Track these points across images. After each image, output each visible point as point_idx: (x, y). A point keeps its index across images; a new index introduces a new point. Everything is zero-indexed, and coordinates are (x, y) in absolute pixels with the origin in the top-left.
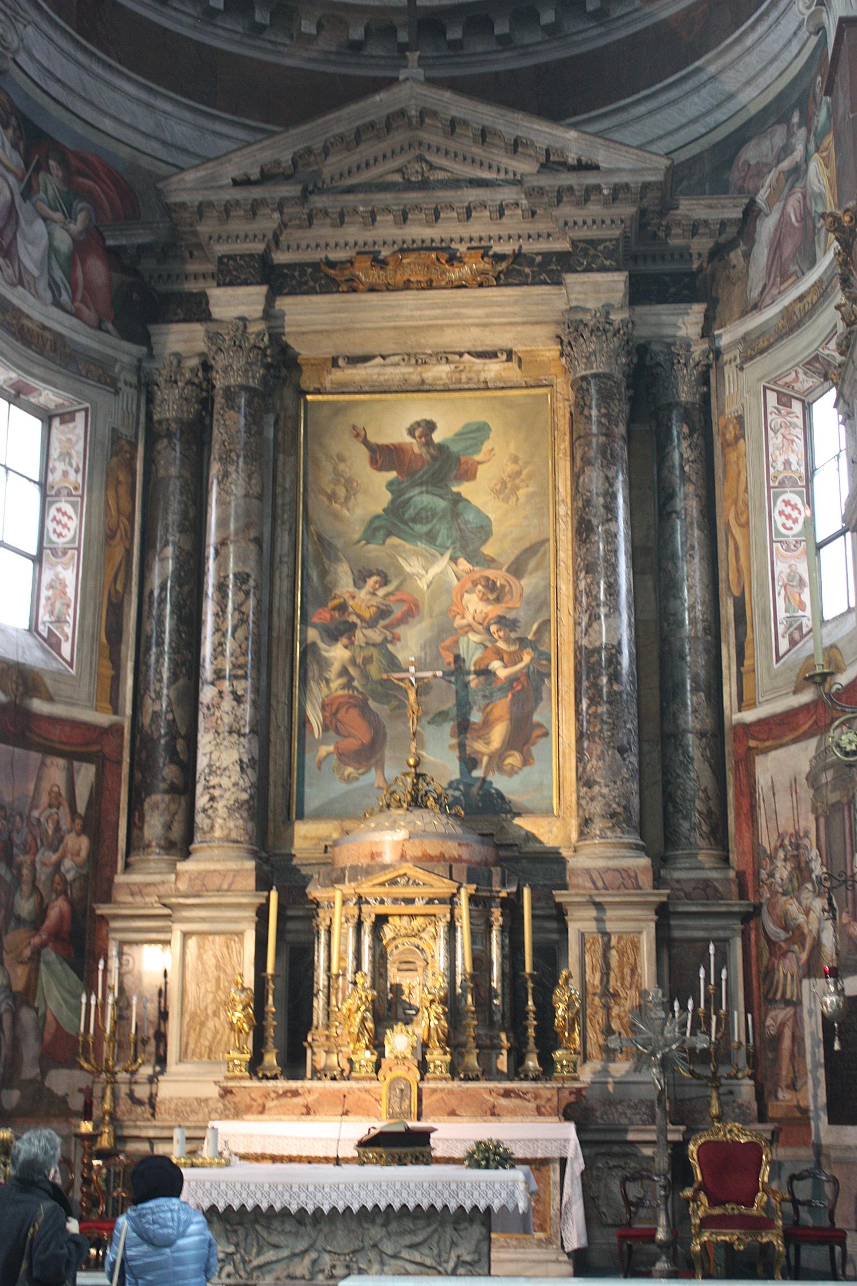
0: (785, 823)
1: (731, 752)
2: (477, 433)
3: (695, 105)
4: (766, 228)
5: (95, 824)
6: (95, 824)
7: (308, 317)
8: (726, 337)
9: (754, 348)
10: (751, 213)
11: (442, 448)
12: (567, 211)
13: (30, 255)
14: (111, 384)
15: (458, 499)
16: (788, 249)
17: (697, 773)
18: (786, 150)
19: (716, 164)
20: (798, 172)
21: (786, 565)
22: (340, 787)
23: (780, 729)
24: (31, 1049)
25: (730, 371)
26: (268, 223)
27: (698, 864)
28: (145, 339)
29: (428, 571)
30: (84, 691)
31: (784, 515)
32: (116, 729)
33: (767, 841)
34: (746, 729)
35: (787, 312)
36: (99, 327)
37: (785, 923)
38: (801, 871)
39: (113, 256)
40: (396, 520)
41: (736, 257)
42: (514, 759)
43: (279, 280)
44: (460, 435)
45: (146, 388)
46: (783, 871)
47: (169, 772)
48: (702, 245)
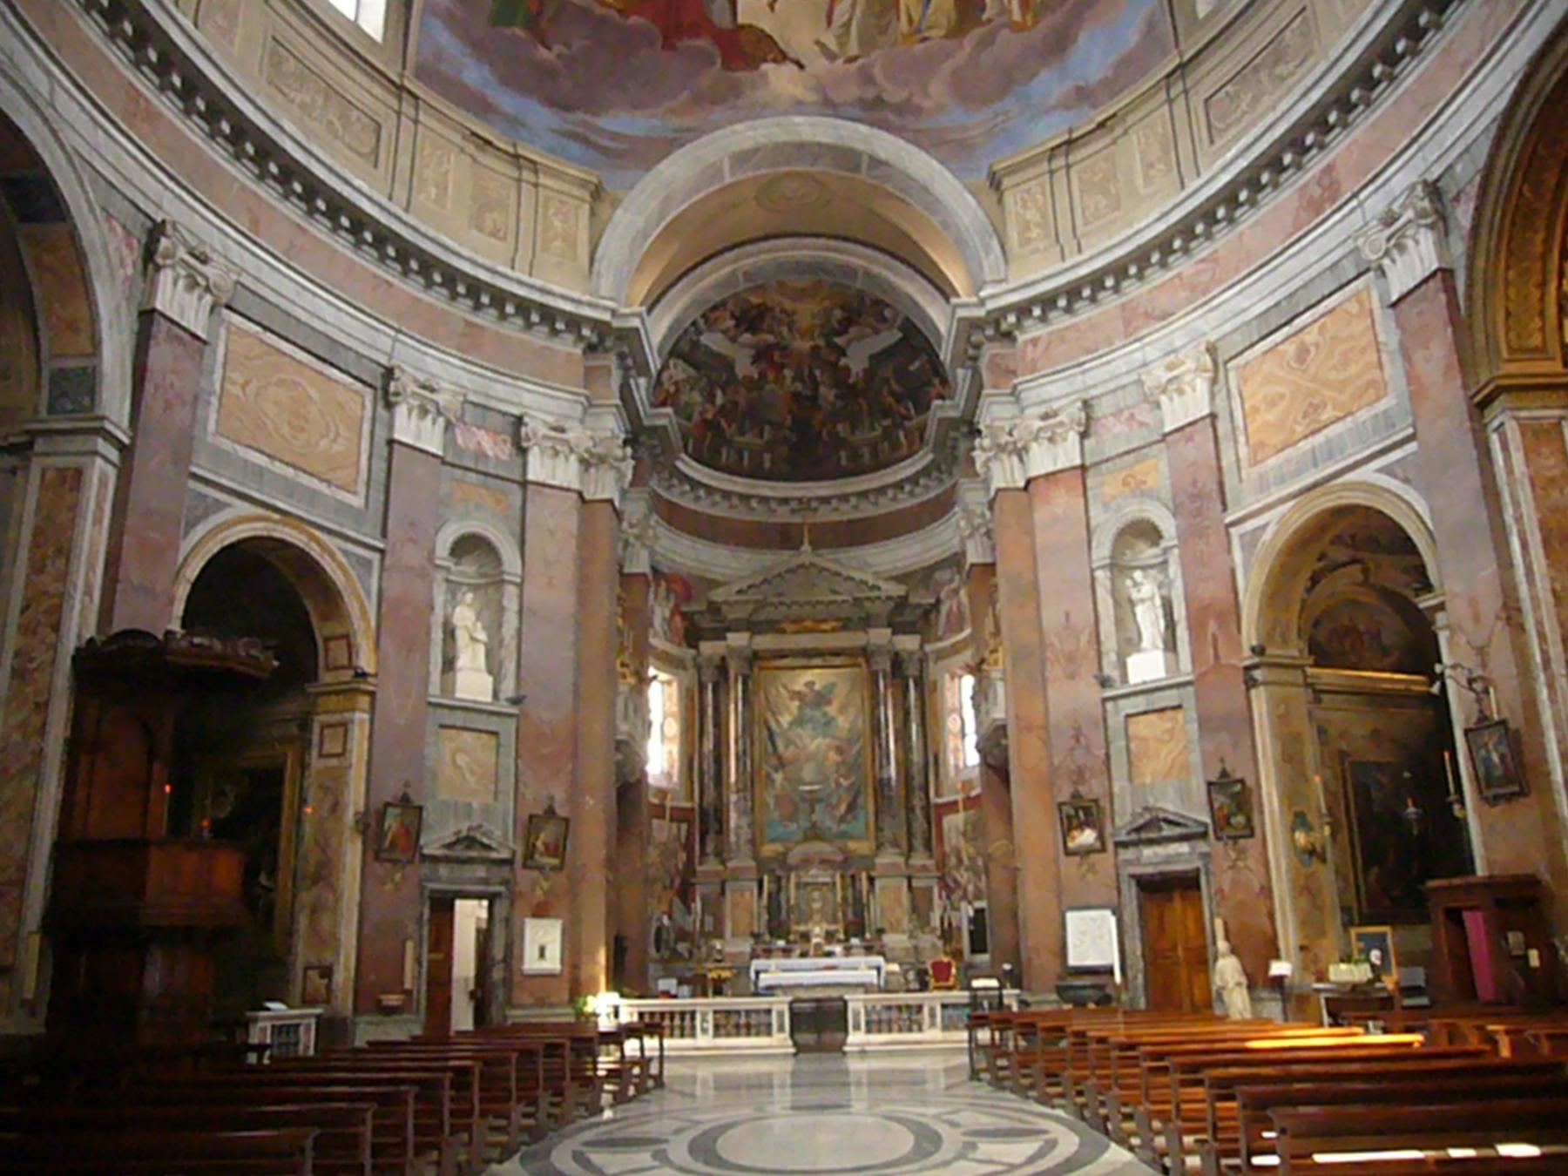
0: (954, 842)
1: (935, 814)
2: (833, 685)
3: (917, 548)
4: (944, 609)
5: (688, 847)
6: (688, 847)
7: (765, 642)
8: (928, 648)
9: (941, 655)
10: (938, 601)
11: (818, 693)
12: (867, 604)
13: (658, 621)
14: (685, 668)
15: (825, 714)
16: (953, 619)
17: (919, 824)
18: (951, 581)
19: (923, 576)
20: (956, 592)
21: (952, 743)
22: (780, 830)
23: (952, 807)
24: (672, 936)
25: (931, 664)
26: (750, 607)
27: (920, 859)
28: (696, 647)
29: (815, 743)
30: (683, 794)
31: (952, 724)
32: (692, 810)
33: (947, 848)
34: (939, 806)
35: (953, 645)
36: (679, 645)
37: (955, 881)
38: (960, 861)
39: (684, 616)
40: (799, 721)
41: (933, 616)
42: (849, 817)
43: (753, 627)
44: (825, 687)
45: (699, 668)
46: (953, 861)
47: (717, 826)
48: (919, 611)
